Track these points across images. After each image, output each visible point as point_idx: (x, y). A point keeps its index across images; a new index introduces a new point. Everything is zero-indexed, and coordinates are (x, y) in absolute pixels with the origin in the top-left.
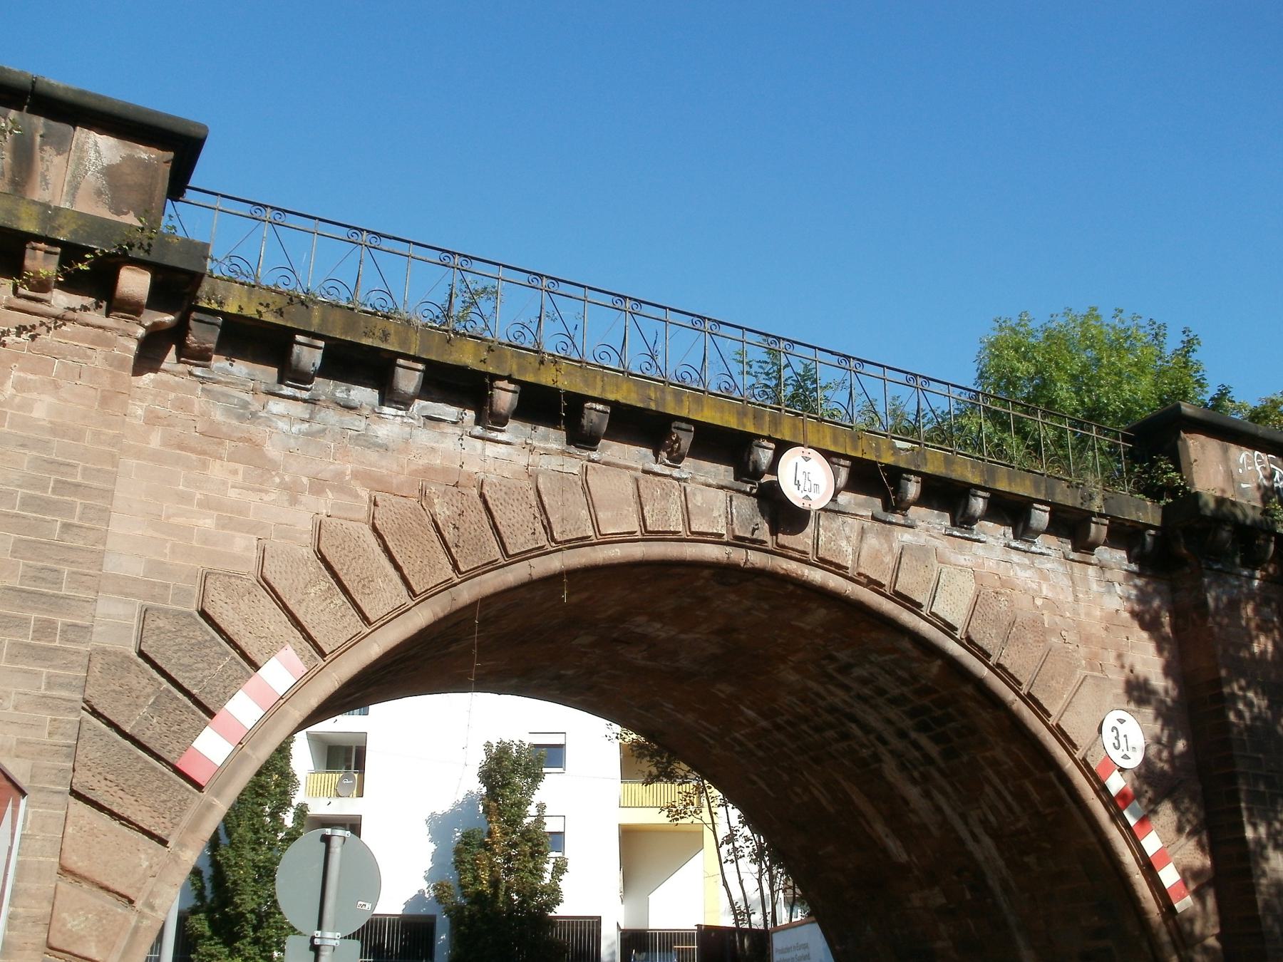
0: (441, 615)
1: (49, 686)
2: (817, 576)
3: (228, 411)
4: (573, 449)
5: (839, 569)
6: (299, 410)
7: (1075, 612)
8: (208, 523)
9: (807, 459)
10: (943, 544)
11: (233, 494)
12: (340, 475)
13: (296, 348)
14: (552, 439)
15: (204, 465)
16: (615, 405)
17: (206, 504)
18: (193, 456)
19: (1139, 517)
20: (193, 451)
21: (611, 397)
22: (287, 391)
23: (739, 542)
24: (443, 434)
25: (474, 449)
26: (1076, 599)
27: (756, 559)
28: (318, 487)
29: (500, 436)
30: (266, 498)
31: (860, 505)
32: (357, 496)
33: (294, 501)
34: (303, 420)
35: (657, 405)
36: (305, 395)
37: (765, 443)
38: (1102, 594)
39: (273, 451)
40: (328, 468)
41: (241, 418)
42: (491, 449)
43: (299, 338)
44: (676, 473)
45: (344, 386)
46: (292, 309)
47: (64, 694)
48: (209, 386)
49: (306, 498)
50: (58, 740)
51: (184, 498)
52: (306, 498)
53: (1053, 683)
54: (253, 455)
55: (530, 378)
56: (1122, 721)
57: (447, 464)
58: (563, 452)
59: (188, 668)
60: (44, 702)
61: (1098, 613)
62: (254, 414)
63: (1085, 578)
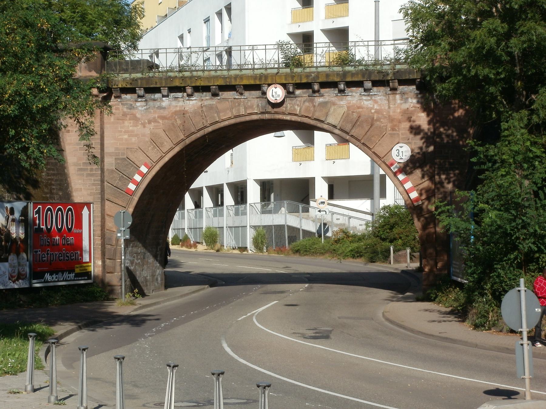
0: (182, 148)
1: (94, 181)
2: (288, 118)
3: (127, 108)
4: (213, 97)
5: (296, 115)
6: (143, 104)
7: (389, 112)
8: (126, 137)
9: (276, 88)
10: (334, 99)
11: (131, 128)
12: (154, 118)
13: (137, 91)
14: (207, 96)
15: (124, 123)
16: (218, 85)
17: (125, 132)
18: (121, 121)
19: (410, 77)
20: (121, 120)
21: (216, 84)
22: (140, 100)
23: (262, 113)
24: (179, 101)
25: (187, 103)
26: (389, 108)
27: (267, 116)
28: (150, 122)
29: (193, 99)
30: (138, 127)
31: (304, 93)
32: (159, 122)
33: (144, 127)
34: (145, 106)
35: (229, 83)
36: (144, 100)
37: (264, 85)
38: (401, 104)
39: (138, 116)
40: (151, 116)
41: (130, 109)
42: (191, 102)
43: (137, 89)
44: (242, 97)
45: (153, 95)
46: (134, 82)
47: (97, 182)
48: (122, 102)
49: (147, 125)
50: (97, 191)
51: (121, 132)
52: (147, 125)
53: (373, 138)
54: (135, 118)
55: (194, 85)
56: (401, 147)
57: (180, 109)
58: (211, 99)
59: (125, 171)
60: (93, 184)
61: (399, 111)
62: (133, 107)
63: (395, 100)
